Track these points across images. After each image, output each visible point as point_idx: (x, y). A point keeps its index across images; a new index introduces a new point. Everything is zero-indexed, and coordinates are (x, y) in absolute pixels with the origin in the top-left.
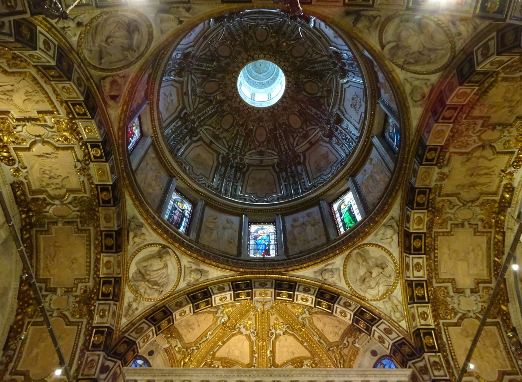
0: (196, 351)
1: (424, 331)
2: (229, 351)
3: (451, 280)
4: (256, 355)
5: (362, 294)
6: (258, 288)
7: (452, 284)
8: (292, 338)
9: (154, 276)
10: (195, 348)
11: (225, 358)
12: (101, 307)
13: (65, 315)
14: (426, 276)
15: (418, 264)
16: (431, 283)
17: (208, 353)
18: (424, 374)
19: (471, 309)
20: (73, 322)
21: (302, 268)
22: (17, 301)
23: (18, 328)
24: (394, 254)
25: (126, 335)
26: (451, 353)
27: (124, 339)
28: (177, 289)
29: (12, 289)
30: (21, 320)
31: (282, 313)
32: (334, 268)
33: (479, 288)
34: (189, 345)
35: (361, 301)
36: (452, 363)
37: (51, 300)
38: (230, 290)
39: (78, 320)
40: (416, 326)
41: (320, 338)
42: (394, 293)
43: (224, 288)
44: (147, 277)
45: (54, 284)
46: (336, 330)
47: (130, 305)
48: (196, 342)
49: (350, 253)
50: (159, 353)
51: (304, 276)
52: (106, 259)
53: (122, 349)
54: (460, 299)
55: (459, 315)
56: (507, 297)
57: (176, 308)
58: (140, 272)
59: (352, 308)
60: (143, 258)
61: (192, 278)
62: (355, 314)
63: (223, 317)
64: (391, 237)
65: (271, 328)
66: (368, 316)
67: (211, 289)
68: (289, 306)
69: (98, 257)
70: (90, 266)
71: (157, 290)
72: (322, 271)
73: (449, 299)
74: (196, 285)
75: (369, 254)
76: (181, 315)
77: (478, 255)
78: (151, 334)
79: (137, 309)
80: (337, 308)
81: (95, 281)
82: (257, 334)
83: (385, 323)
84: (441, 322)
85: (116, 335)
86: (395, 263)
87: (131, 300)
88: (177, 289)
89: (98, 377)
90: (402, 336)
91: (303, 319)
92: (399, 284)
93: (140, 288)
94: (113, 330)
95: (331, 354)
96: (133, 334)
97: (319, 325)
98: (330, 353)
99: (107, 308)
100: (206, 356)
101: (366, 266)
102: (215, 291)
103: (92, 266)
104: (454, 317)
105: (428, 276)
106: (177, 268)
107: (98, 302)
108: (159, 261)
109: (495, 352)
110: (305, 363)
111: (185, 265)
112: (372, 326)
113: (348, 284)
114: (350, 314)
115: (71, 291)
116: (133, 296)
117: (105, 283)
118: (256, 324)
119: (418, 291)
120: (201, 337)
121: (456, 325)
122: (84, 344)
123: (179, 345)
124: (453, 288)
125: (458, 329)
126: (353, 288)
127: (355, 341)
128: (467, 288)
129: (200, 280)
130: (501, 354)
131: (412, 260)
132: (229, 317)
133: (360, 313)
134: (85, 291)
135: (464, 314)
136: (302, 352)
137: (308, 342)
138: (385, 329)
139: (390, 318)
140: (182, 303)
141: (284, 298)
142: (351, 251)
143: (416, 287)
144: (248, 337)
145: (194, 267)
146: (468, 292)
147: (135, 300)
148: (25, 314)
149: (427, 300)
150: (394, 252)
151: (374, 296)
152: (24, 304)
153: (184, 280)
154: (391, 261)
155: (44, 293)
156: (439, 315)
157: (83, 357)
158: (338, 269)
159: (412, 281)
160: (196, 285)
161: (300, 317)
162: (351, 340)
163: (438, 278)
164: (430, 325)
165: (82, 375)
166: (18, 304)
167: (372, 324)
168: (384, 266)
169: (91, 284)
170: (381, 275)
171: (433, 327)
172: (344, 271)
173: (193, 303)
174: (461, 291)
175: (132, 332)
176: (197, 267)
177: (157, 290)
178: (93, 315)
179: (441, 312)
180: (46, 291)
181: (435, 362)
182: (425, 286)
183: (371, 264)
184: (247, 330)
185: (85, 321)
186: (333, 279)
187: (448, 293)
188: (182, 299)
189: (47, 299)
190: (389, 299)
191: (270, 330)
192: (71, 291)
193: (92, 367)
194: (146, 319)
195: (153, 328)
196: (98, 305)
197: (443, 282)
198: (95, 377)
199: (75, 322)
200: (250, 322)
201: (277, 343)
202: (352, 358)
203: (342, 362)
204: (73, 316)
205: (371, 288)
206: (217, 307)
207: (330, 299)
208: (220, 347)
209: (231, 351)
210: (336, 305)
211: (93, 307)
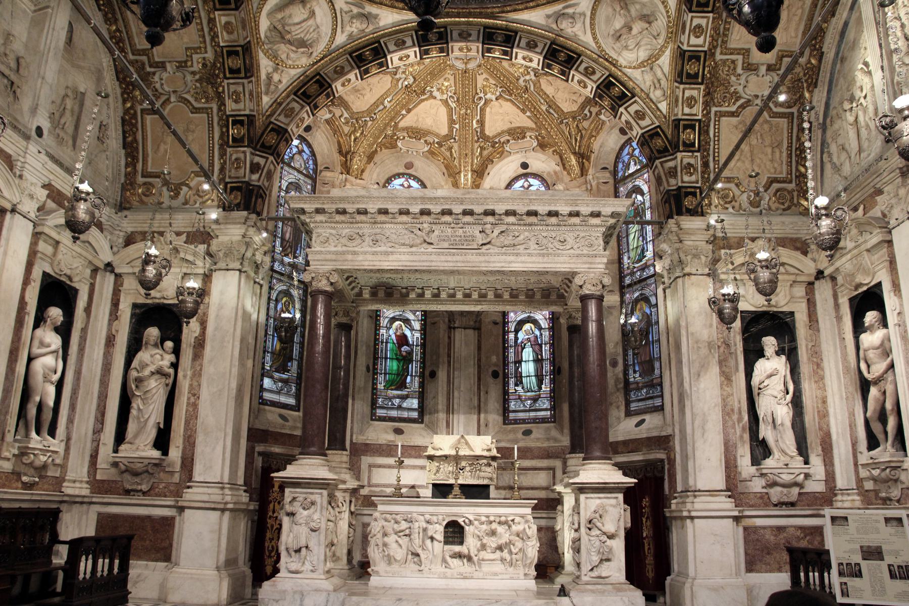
0: (370, 123)
1: (686, 123)
2: (417, 120)
4: (457, 126)
5: (615, 57)
6: (457, 41)
8: (509, 104)
9: (297, 32)
10: (368, 119)
11: (411, 127)
12: (233, 88)
13: (186, 99)
14: (707, 44)
15: (699, 26)
16: (713, 55)
17: (386, 125)
18: (671, 177)
19: (760, 94)
20: (199, 109)
21: (526, 8)
22: (117, 83)
23: (131, 118)
25: (272, 120)
26: (714, 152)
27: (271, 126)
28: (333, 46)
29: (106, 69)
30: (132, 107)
31: (494, 72)
33: (781, 64)
34: (360, 115)
36: (711, 165)
37: (162, 79)
38: (414, 45)
39: (206, 105)
40: (676, 115)
41: (550, 106)
42: (660, 62)
43: (404, 42)
44: (288, 37)
45: (158, 57)
46: (575, 98)
47: (269, 78)
48: (370, 111)
50: (319, 127)
51: (529, 21)
52: (224, 20)
53: (271, 139)
54: (749, 79)
55: (742, 101)
56: (817, 80)
57: (336, 76)
58: (275, 27)
59: (595, 78)
60: (276, 5)
61: (356, 27)
62: (598, 87)
63: (406, 79)
65: (478, 91)
66: (616, 91)
67: (385, 44)
68: (505, 64)
69: (212, 16)
70: (202, 30)
71: (303, 53)
72: (559, 16)
73: (733, 78)
74: (360, 38)
76: (343, 85)
77: (794, 15)
78: (305, 115)
79: (280, 81)
80: (573, 75)
81: (216, 51)
82: (458, 99)
84: (714, 109)
85: (260, 122)
86: (669, 17)
87: (270, 70)
88: (333, 46)
89: (250, 179)
90: (658, 124)
91: (525, 81)
93: (279, 53)
94: (254, 116)
95: (564, 128)
96: (282, 118)
97: (549, 90)
98: (563, 126)
99: (240, 89)
100: (385, 128)
102: (392, 47)
103: (206, 30)
104: (734, 104)
106: (329, 13)
107: (226, 81)
108: (300, 6)
109: (773, 152)
110: (528, 134)
111: (341, 9)
112: (620, 106)
113: (595, 38)
114: (591, 86)
115: (187, 67)
116: (271, 63)
117: (230, 54)
118: (455, 86)
120: (376, 104)
121: (732, 114)
122: (221, 137)
123: (346, 115)
124: (743, 63)
125: (734, 120)
126: (603, 45)
127: (600, 111)
128: (763, 64)
129: (367, 30)
130: (781, 156)
131: (692, 20)
132: (414, 78)
133: (606, 86)
134: (204, 65)
135: (749, 101)
136: (523, 120)
137: (532, 112)
138: (636, 112)
139: (648, 95)
140: (343, 68)
141: (497, 54)
144: (445, 103)
145: (355, 10)
146: (763, 69)
147: (276, 70)
148: (133, 99)
149: (700, 80)
151: (630, 62)
152: (127, 86)
153: (342, 32)
155: (148, 69)
156: (712, 99)
157: (225, 154)
158: (584, 14)
159: (685, 51)
160: (360, 38)
161: (521, 81)
162: (594, 110)
164: (695, 115)
165: (230, 177)
166: (121, 87)
167: (620, 103)
168: (652, 19)
169: (210, 55)
171: (700, 117)
172: (592, 18)
173: (359, 68)
174: (753, 68)
175: (279, 115)
176: (361, 10)
177: (303, 53)
178: (224, 98)
179: (718, 96)
180: (151, 66)
181: (689, 164)
183: (633, 12)
184: (443, 93)
185: (215, 107)
186: (574, 29)
187: (735, 69)
188: (341, 62)
189: (156, 78)
190: (651, 69)
191: (477, 94)
192: (187, 67)
193: (238, 168)
194: (295, 94)
195: (308, 108)
196: (228, 86)
197: (731, 54)
198: (247, 179)
199: (203, 108)
200: (446, 84)
201: (488, 109)
202: (594, 134)
203: (578, 138)
204: (196, 99)
206: (397, 68)
207: (565, 61)
208: (404, 116)
209: (420, 119)
210: (572, 72)
211: (221, 89)
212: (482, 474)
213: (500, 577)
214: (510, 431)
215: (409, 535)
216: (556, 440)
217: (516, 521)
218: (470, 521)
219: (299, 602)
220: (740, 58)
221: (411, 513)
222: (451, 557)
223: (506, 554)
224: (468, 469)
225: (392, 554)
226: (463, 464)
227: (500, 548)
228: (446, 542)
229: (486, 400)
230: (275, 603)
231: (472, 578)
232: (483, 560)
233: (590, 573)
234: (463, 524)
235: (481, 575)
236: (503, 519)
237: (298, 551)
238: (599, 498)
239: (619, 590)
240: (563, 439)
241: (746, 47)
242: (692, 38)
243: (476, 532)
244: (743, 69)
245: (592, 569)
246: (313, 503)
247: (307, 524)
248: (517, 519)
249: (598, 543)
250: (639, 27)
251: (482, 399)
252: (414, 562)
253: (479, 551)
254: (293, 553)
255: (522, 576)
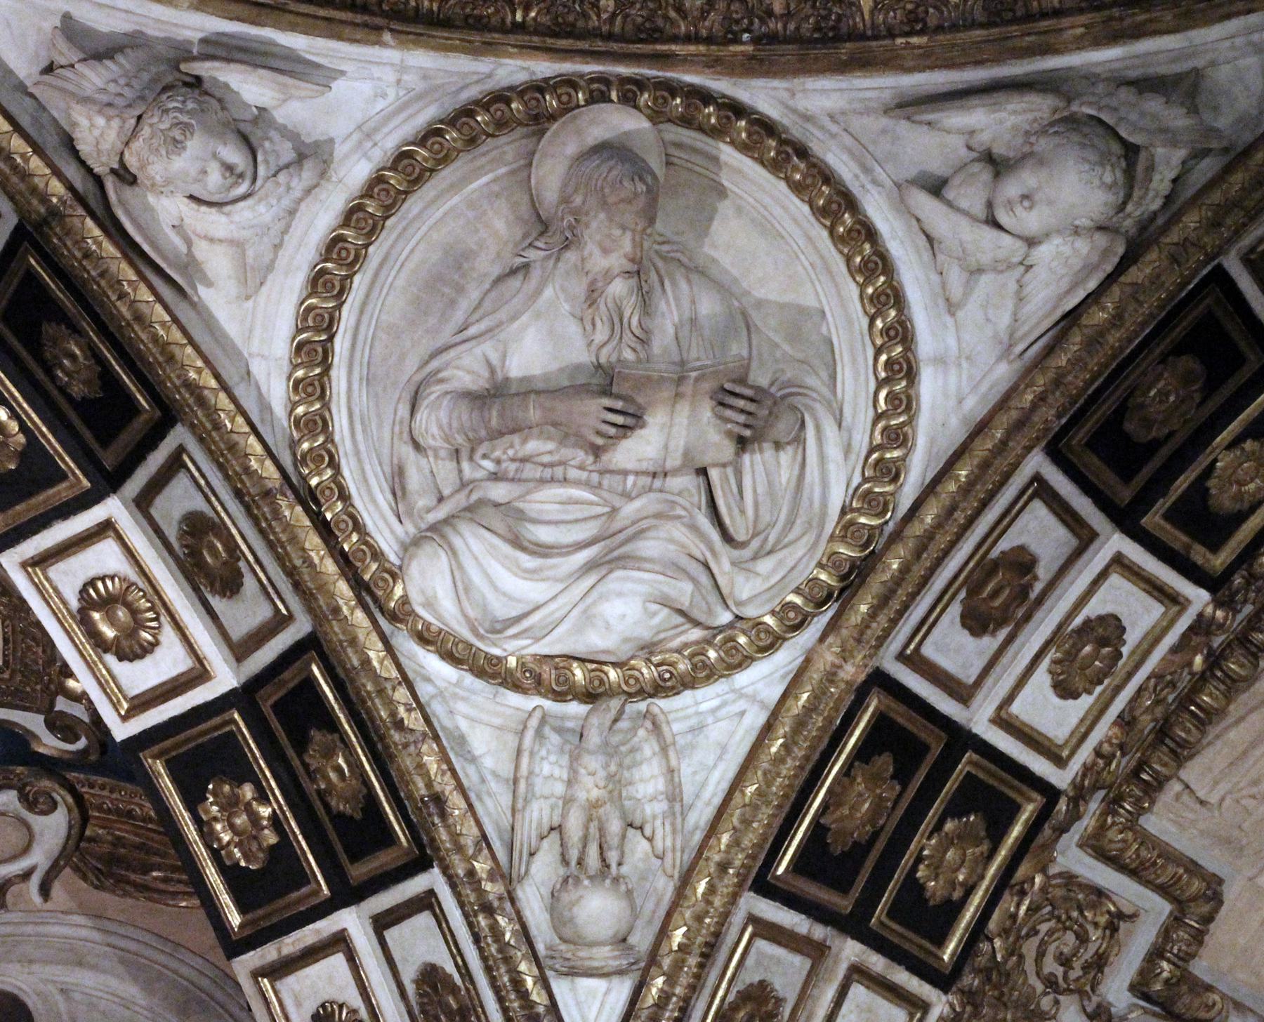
3: (1196, 885)
7: (1177, 920)
14: (1085, 754)
24: (929, 386)
32: (280, 116)
35: (343, 588)
49: (539, 87)
64: (1031, 242)
75: (703, 221)
83: (441, 919)
92: (786, 658)
101: (617, 320)
105: (1087, 769)
119: (949, 842)
124: (1156, 953)
131: (1103, 576)
142: (570, 82)
143: (954, 810)
150: (940, 361)
154: (862, 433)
163: (1131, 824)
170: (686, 482)
182: (1016, 831)
187: (1099, 963)
197: (1134, 873)
205: (517, 542)
220: (1157, 908)
241: (1212, 861)
242: (1042, 677)
244: (1139, 988)
250: (679, 444)
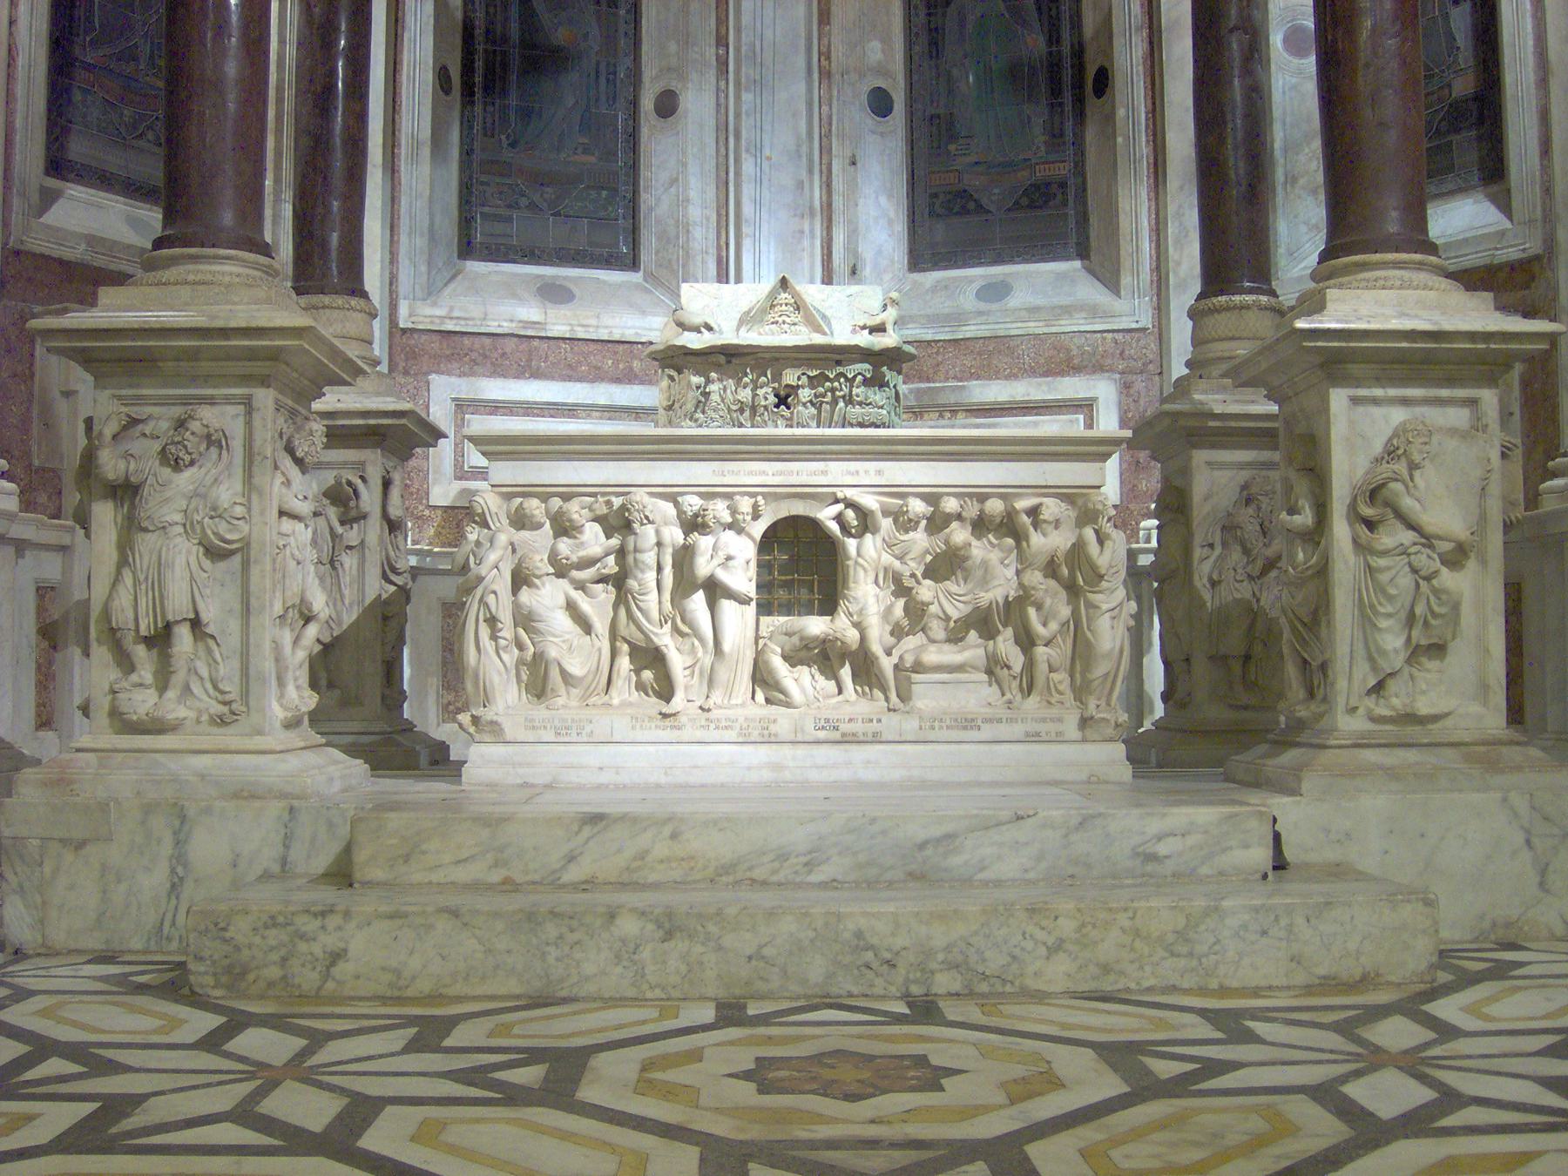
212: (855, 412)
213: (987, 732)
214: (935, 289)
215: (618, 580)
216: (1094, 312)
217: (1046, 514)
218: (863, 513)
219: (167, 848)
221: (624, 489)
222: (791, 659)
223: (1006, 644)
224: (805, 394)
225: (553, 653)
226: (790, 377)
227: (982, 622)
228: (765, 608)
229: (852, 186)
230: (69, 857)
231: (876, 739)
232: (918, 667)
233: (1370, 702)
234: (834, 527)
235: (910, 726)
236: (995, 506)
237: (160, 639)
238: (1405, 402)
239: (1493, 765)
240: (1119, 305)
243: (887, 559)
245: (1379, 688)
246: (216, 441)
247: (188, 527)
248: (1052, 508)
249: (1406, 581)
251: (838, 184)
252: (641, 686)
253: (898, 632)
254: (140, 651)
255: (1071, 728)
